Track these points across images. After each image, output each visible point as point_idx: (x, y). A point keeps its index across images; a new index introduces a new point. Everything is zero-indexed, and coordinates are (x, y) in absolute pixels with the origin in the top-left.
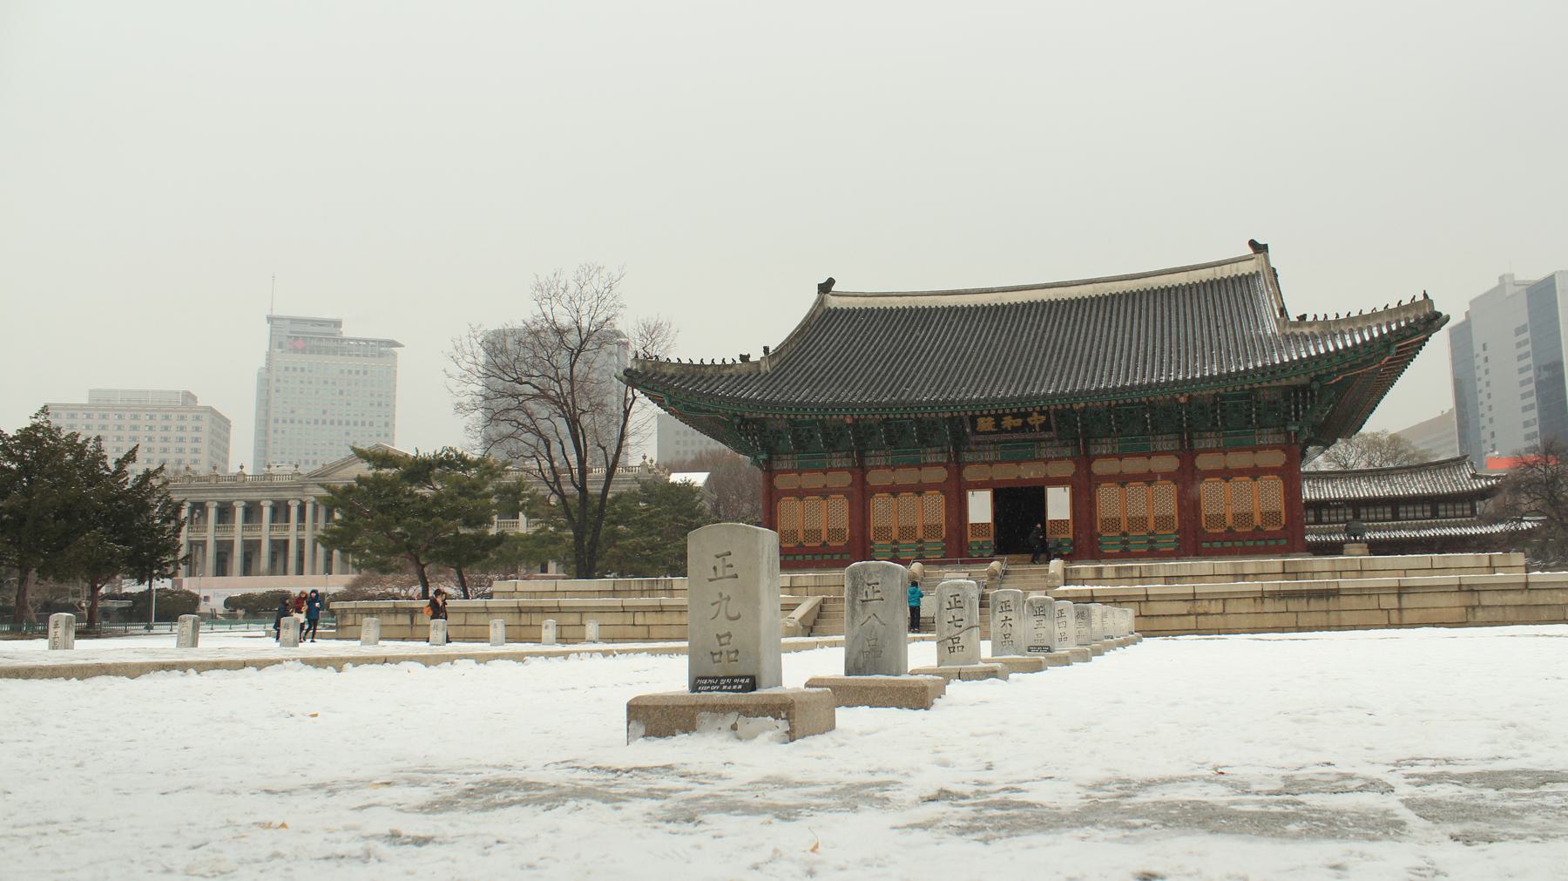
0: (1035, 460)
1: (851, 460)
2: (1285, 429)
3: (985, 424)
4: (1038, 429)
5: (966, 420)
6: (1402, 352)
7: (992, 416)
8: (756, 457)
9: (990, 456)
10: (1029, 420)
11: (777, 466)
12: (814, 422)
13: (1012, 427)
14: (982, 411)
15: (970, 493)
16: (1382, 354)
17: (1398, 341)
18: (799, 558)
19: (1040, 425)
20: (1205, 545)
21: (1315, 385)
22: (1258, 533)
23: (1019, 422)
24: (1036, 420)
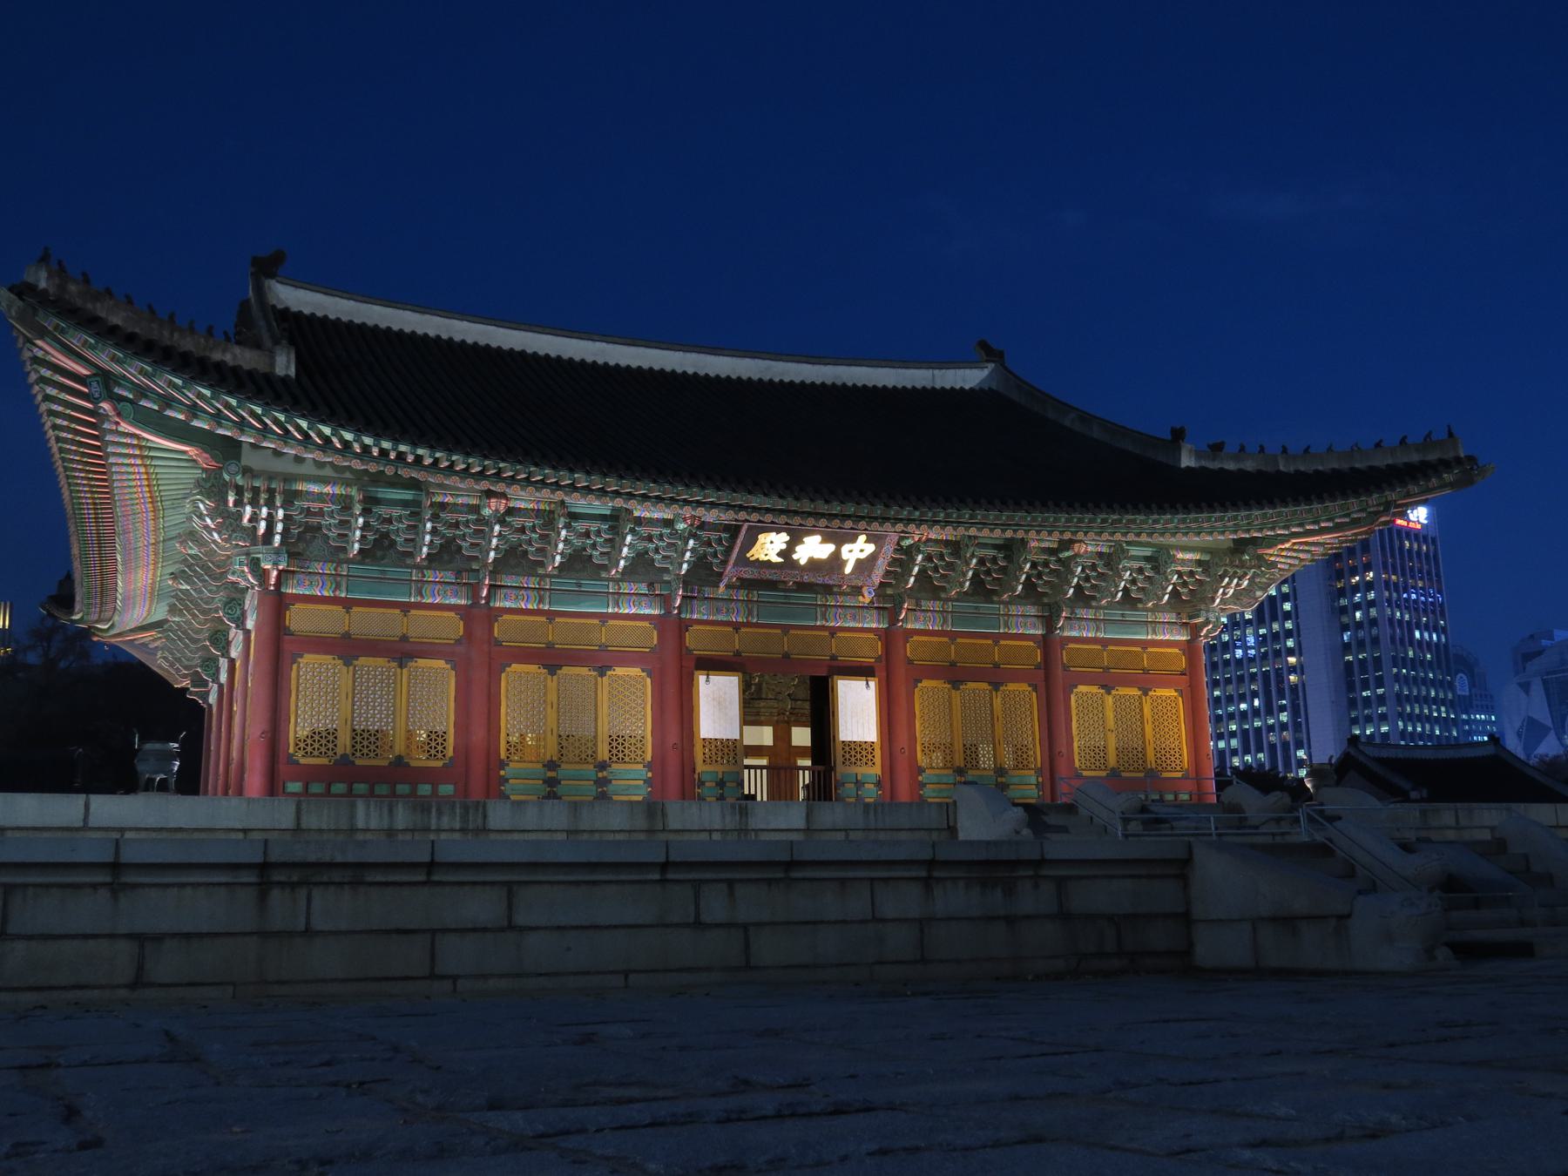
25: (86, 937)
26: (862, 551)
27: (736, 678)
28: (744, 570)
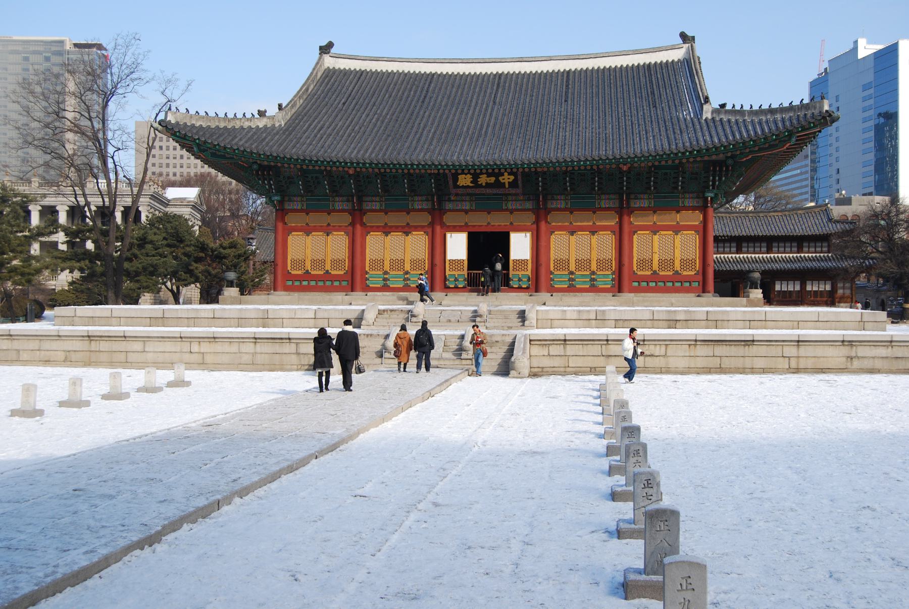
0: (503, 210)
1: (350, 204)
2: (704, 195)
3: (465, 180)
4: (507, 186)
5: (449, 176)
6: (801, 140)
7: (471, 174)
8: (270, 198)
9: (467, 206)
10: (500, 178)
11: (287, 206)
12: (321, 172)
13: (487, 183)
14: (463, 170)
16: (784, 141)
17: (799, 132)
18: (305, 283)
19: (509, 182)
20: (636, 284)
21: (730, 162)
22: (677, 277)
23: (492, 179)
24: (507, 179)
25: (55, 351)
26: (509, 179)
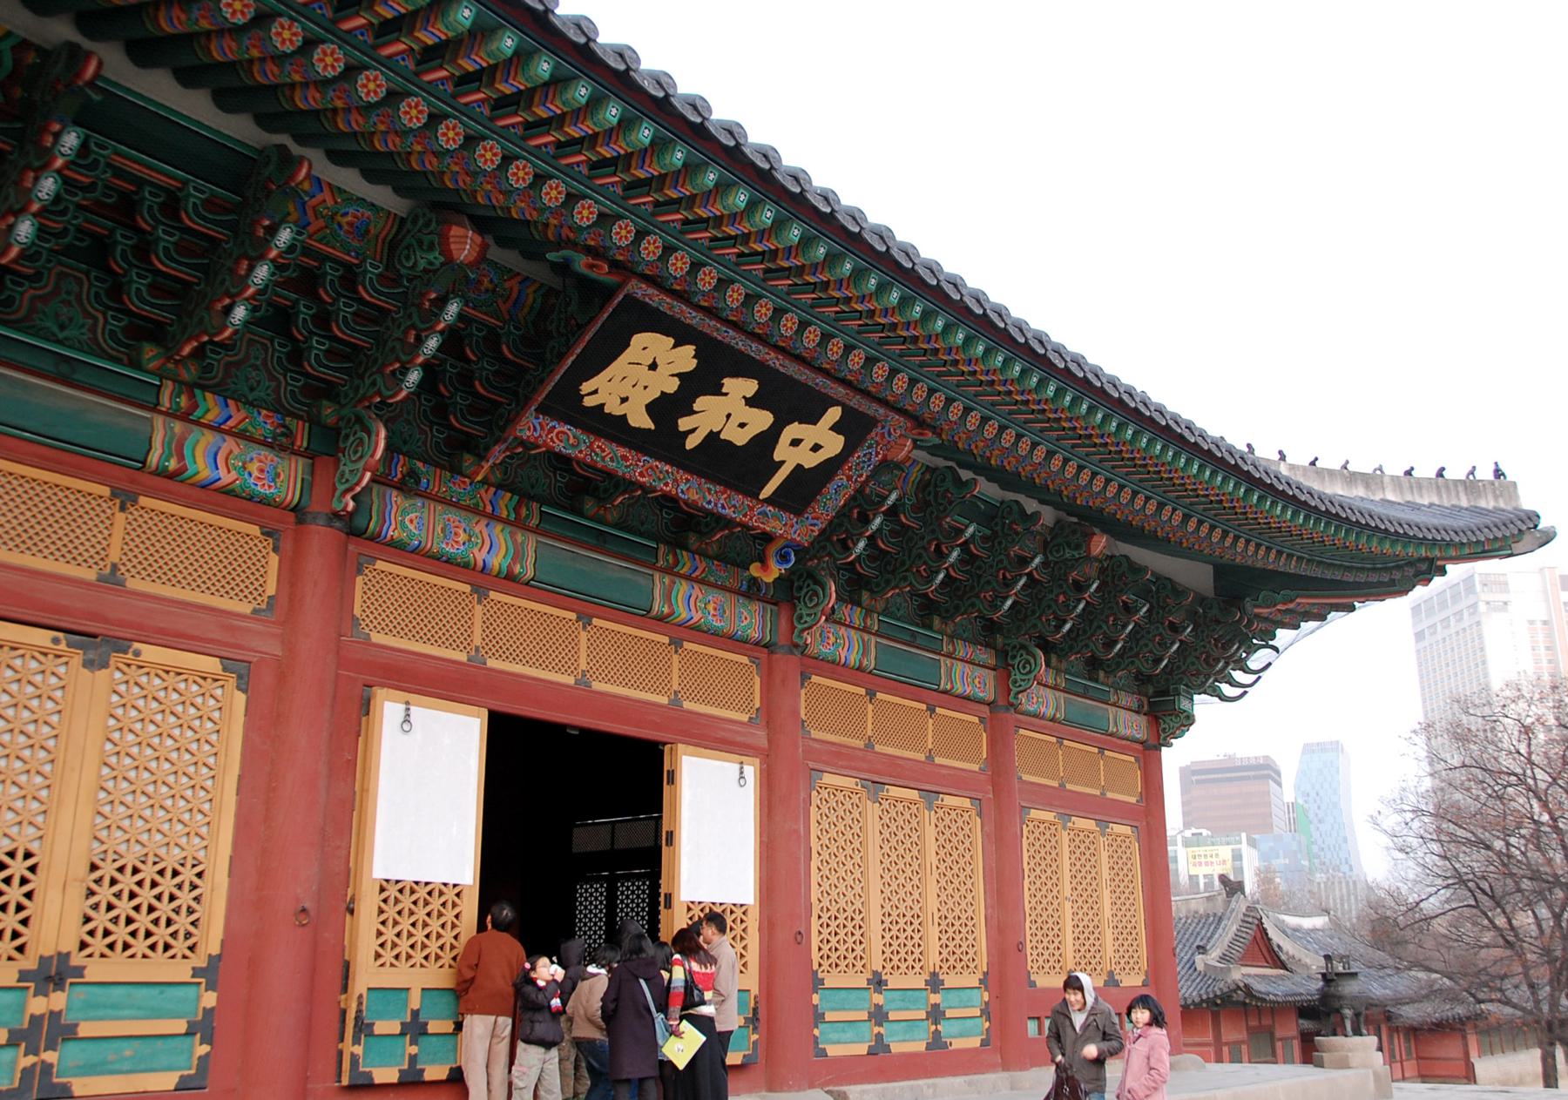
15: (390, 709)
27: (478, 721)
28: (559, 429)
